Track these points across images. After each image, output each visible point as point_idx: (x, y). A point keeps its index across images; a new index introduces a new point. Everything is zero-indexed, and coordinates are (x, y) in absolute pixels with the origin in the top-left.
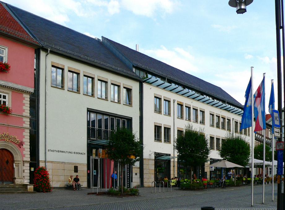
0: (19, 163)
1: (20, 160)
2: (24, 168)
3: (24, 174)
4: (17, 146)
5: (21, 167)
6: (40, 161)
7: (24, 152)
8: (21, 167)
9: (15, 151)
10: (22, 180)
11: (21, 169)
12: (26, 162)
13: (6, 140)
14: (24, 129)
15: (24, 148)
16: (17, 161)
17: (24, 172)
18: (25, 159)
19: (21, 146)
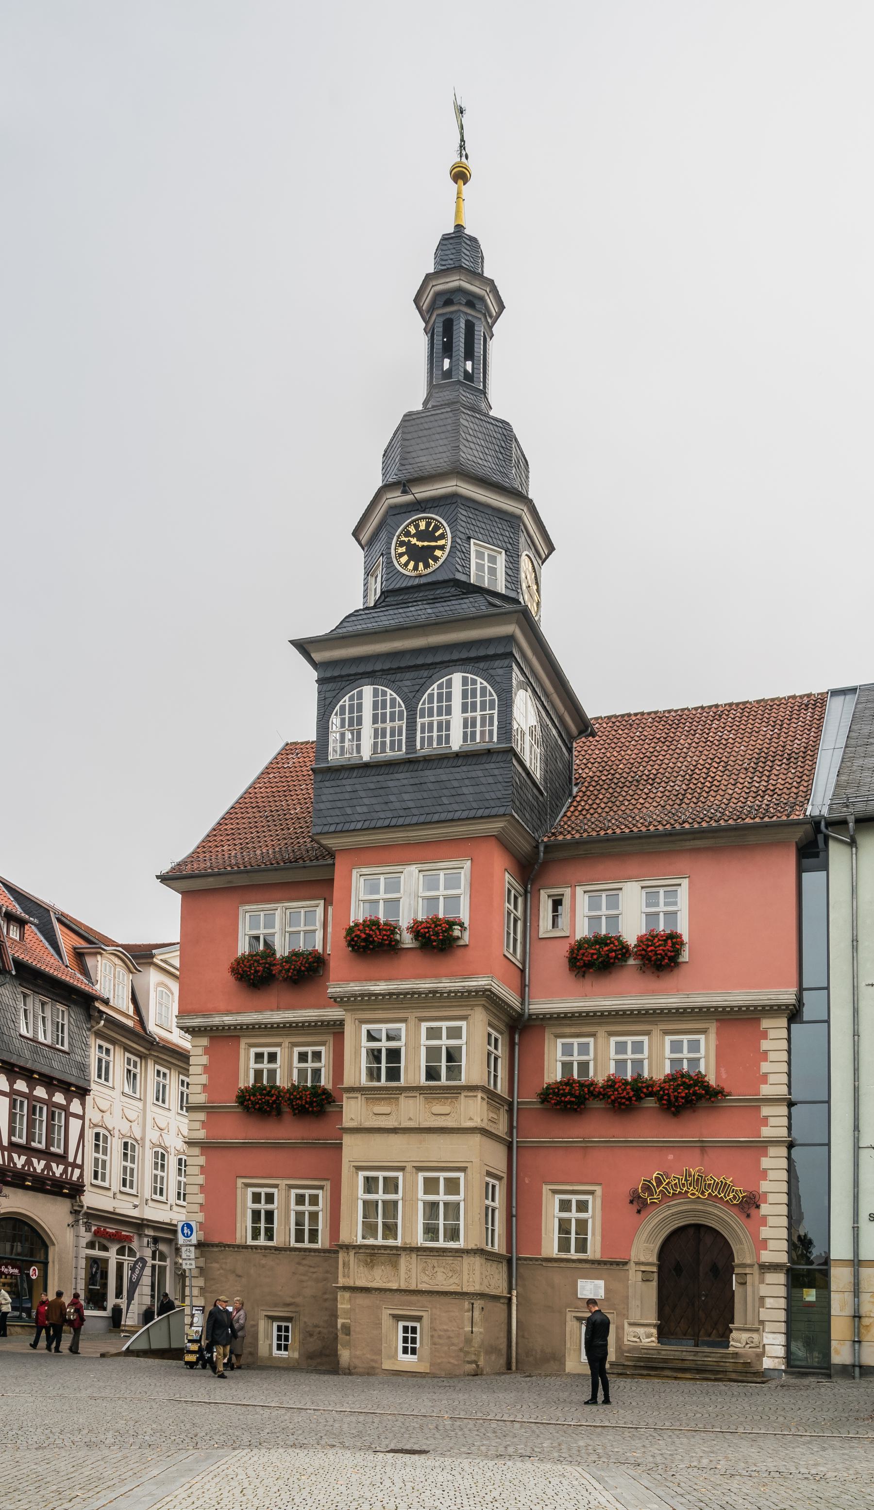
0: (746, 1274)
1: (749, 1262)
2: (764, 1290)
3: (764, 1315)
4: (736, 1210)
5: (753, 1286)
6: (832, 1262)
7: (765, 1232)
8: (753, 1286)
9: (733, 1229)
10: (755, 1336)
11: (753, 1292)
12: (774, 1267)
13: (693, 1194)
14: (763, 1146)
15: (765, 1217)
16: (740, 1266)
17: (762, 1304)
18: (766, 1257)
19: (753, 1211)
